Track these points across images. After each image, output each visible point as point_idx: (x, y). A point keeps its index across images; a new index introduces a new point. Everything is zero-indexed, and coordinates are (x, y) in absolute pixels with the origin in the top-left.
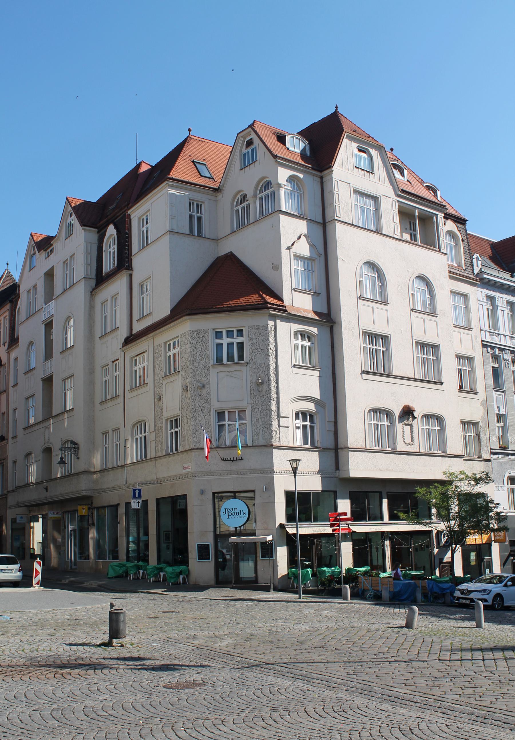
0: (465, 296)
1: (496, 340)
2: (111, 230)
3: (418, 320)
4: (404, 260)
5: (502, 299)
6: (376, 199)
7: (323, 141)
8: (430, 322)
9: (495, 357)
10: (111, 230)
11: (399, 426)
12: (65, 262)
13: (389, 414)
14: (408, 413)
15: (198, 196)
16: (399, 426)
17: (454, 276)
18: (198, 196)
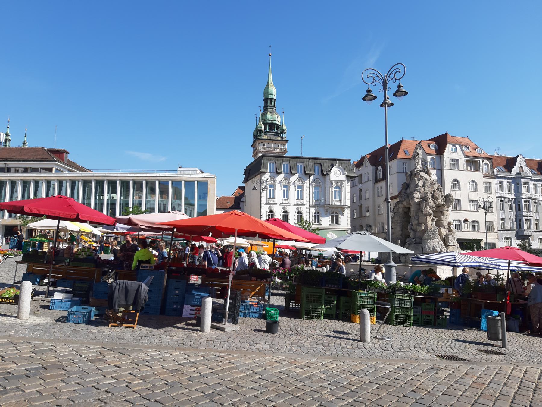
0: (490, 183)
1: (502, 195)
2: (380, 167)
3: (471, 194)
4: (466, 176)
5: (505, 182)
6: (458, 160)
7: (441, 142)
8: (475, 194)
9: (501, 201)
10: (380, 167)
11: (463, 224)
12: (365, 174)
13: (460, 221)
14: (466, 221)
15: (405, 162)
16: (463, 224)
17: (485, 176)
18: (405, 162)
